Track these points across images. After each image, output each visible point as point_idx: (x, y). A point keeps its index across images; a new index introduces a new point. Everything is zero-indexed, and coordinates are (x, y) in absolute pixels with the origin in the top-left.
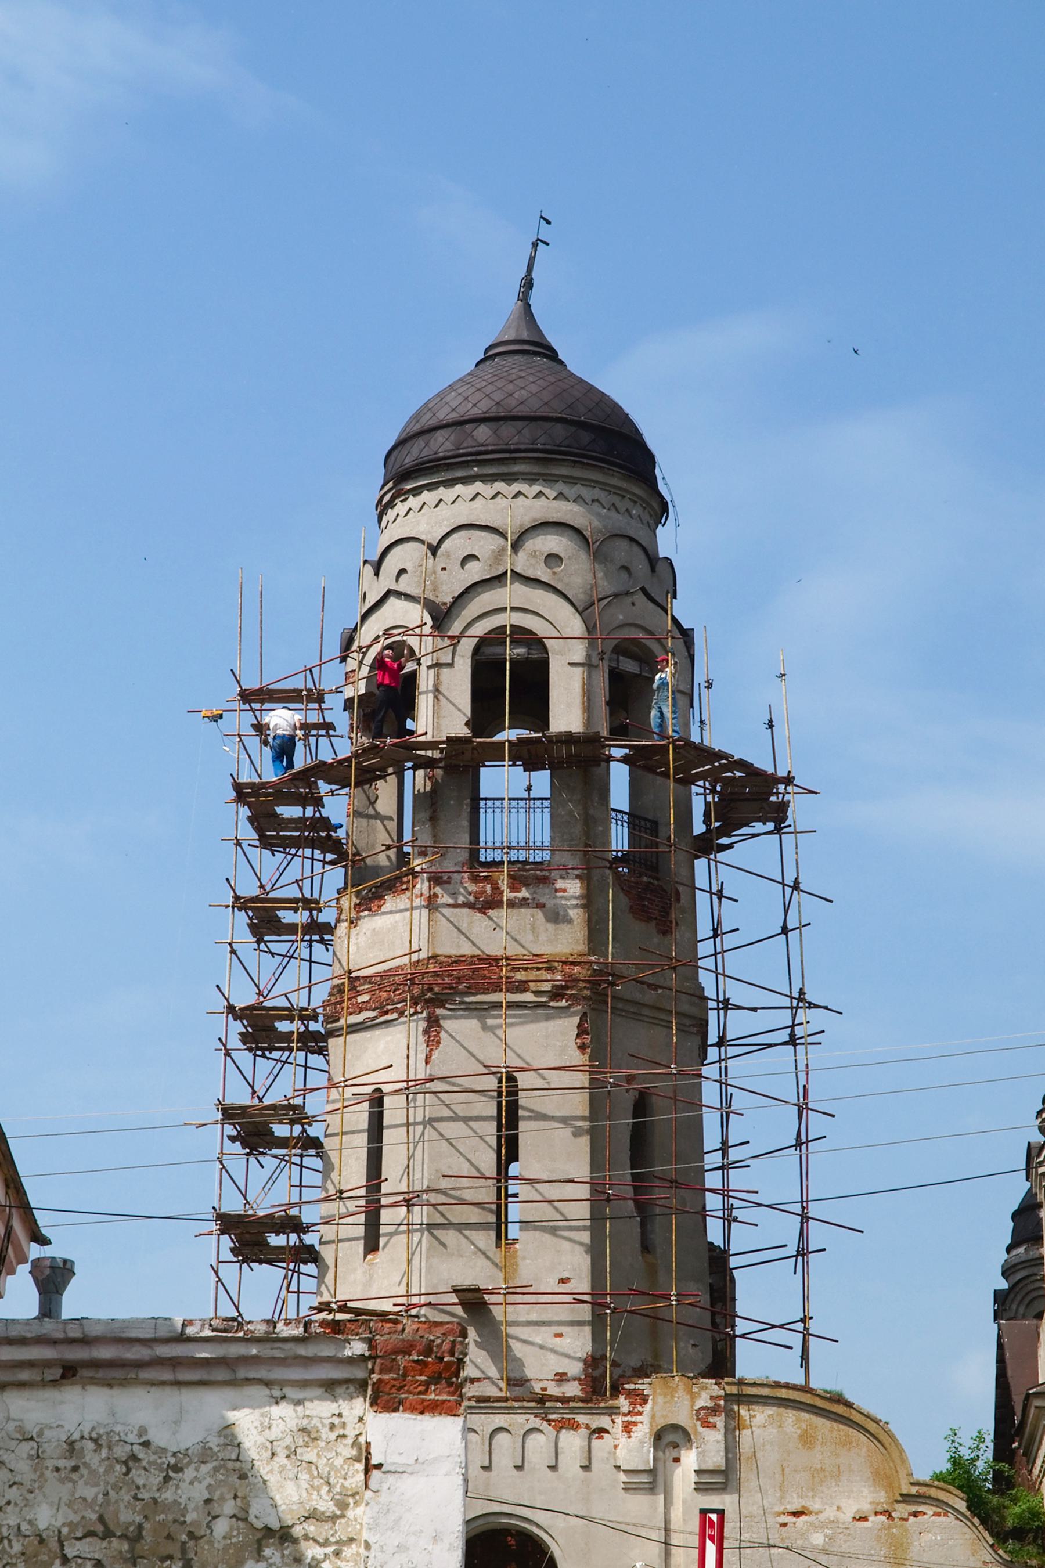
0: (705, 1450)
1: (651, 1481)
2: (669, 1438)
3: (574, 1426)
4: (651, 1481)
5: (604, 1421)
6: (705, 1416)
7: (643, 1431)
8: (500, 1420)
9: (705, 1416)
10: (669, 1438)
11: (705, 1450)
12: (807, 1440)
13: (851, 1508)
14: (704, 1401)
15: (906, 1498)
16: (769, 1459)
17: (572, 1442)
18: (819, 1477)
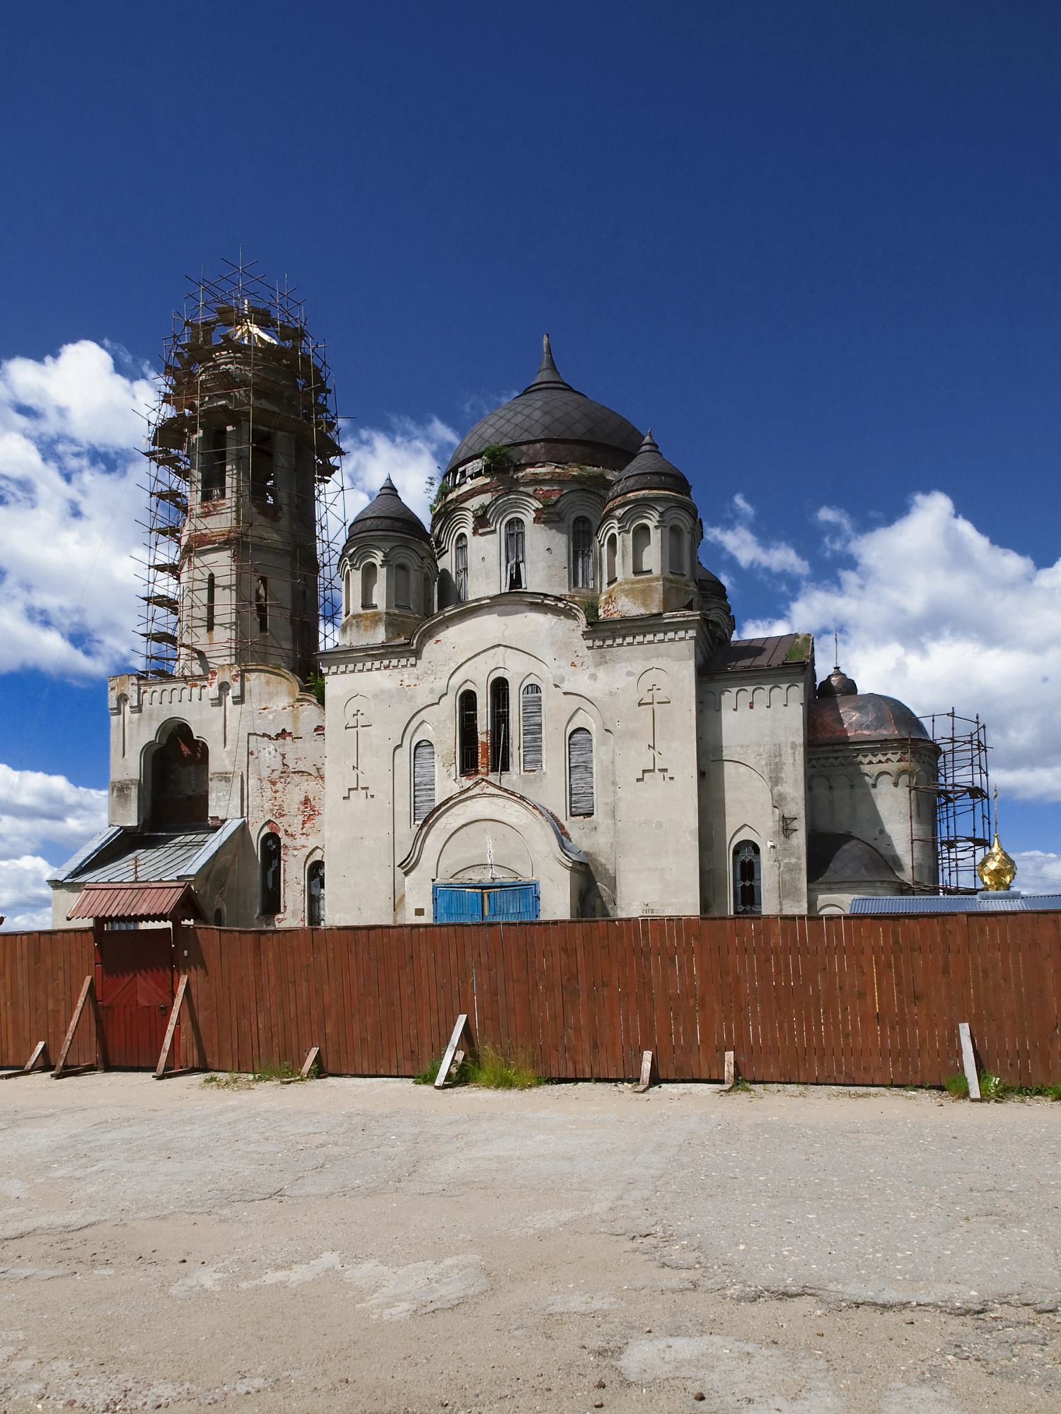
0: (235, 690)
1: (219, 702)
2: (224, 687)
3: (196, 685)
4: (219, 702)
5: (205, 683)
6: (234, 678)
7: (215, 685)
8: (174, 686)
9: (234, 678)
10: (224, 687)
11: (235, 690)
12: (268, 683)
13: (281, 705)
14: (234, 673)
15: (298, 700)
16: (256, 691)
17: (196, 691)
18: (272, 696)
